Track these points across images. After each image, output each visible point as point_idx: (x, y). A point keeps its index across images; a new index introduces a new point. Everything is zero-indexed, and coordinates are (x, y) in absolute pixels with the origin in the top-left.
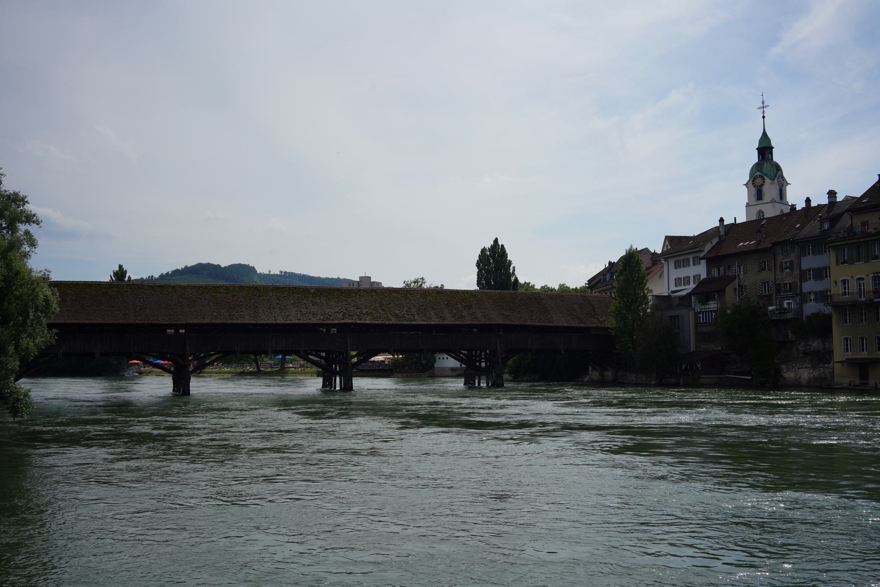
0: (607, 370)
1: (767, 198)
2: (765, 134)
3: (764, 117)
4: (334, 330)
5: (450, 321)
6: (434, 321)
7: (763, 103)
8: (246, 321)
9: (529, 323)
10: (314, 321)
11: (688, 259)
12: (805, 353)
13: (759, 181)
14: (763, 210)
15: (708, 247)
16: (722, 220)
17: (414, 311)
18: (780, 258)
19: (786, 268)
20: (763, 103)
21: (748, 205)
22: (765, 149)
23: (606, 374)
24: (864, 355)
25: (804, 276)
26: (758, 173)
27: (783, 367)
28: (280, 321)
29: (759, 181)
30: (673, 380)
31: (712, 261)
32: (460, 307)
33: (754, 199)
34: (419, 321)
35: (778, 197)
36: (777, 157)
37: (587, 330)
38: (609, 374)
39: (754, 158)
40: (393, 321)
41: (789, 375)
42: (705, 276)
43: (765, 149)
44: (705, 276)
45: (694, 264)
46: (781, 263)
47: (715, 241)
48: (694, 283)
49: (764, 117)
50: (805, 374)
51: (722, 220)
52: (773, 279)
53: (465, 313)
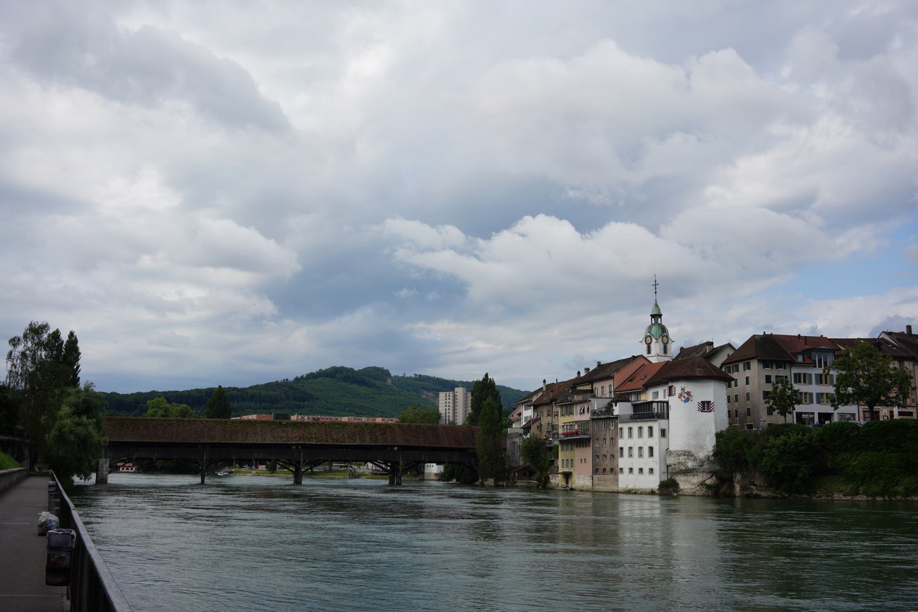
1: (653, 352)
2: (657, 305)
4: (294, 447)
5: (368, 442)
6: (358, 443)
8: (240, 441)
9: (422, 445)
10: (280, 442)
15: (535, 398)
16: (544, 381)
17: (346, 436)
22: (656, 316)
24: (567, 470)
28: (260, 442)
30: (501, 483)
31: (536, 407)
32: (378, 433)
34: (348, 443)
35: (662, 352)
36: (665, 321)
37: (466, 449)
40: (330, 442)
43: (656, 316)
47: (540, 394)
51: (544, 381)
53: (380, 438)
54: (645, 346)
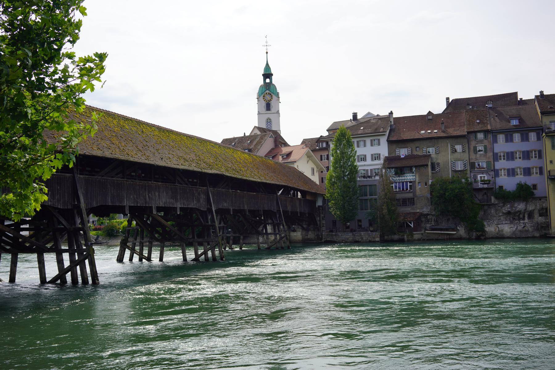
0: (294, 231)
2: (267, 64)
3: (267, 53)
7: (266, 42)
11: (365, 141)
12: (509, 213)
13: (268, 97)
14: (271, 118)
18: (473, 144)
19: (480, 151)
20: (266, 42)
21: (259, 113)
23: (293, 234)
25: (496, 157)
26: (267, 91)
27: (485, 223)
29: (268, 97)
33: (264, 110)
38: (297, 235)
39: (260, 81)
41: (490, 229)
42: (387, 155)
43: (268, 75)
44: (387, 155)
45: (372, 145)
46: (475, 148)
48: (372, 160)
49: (267, 53)
50: (507, 229)
52: (468, 159)
54: (264, 104)
